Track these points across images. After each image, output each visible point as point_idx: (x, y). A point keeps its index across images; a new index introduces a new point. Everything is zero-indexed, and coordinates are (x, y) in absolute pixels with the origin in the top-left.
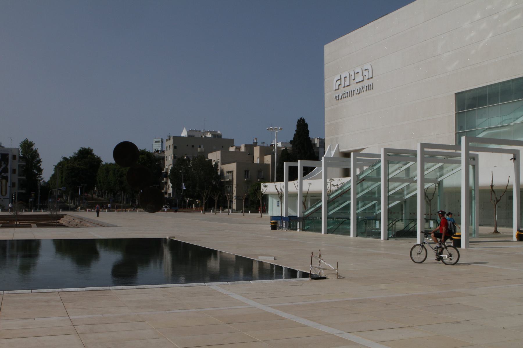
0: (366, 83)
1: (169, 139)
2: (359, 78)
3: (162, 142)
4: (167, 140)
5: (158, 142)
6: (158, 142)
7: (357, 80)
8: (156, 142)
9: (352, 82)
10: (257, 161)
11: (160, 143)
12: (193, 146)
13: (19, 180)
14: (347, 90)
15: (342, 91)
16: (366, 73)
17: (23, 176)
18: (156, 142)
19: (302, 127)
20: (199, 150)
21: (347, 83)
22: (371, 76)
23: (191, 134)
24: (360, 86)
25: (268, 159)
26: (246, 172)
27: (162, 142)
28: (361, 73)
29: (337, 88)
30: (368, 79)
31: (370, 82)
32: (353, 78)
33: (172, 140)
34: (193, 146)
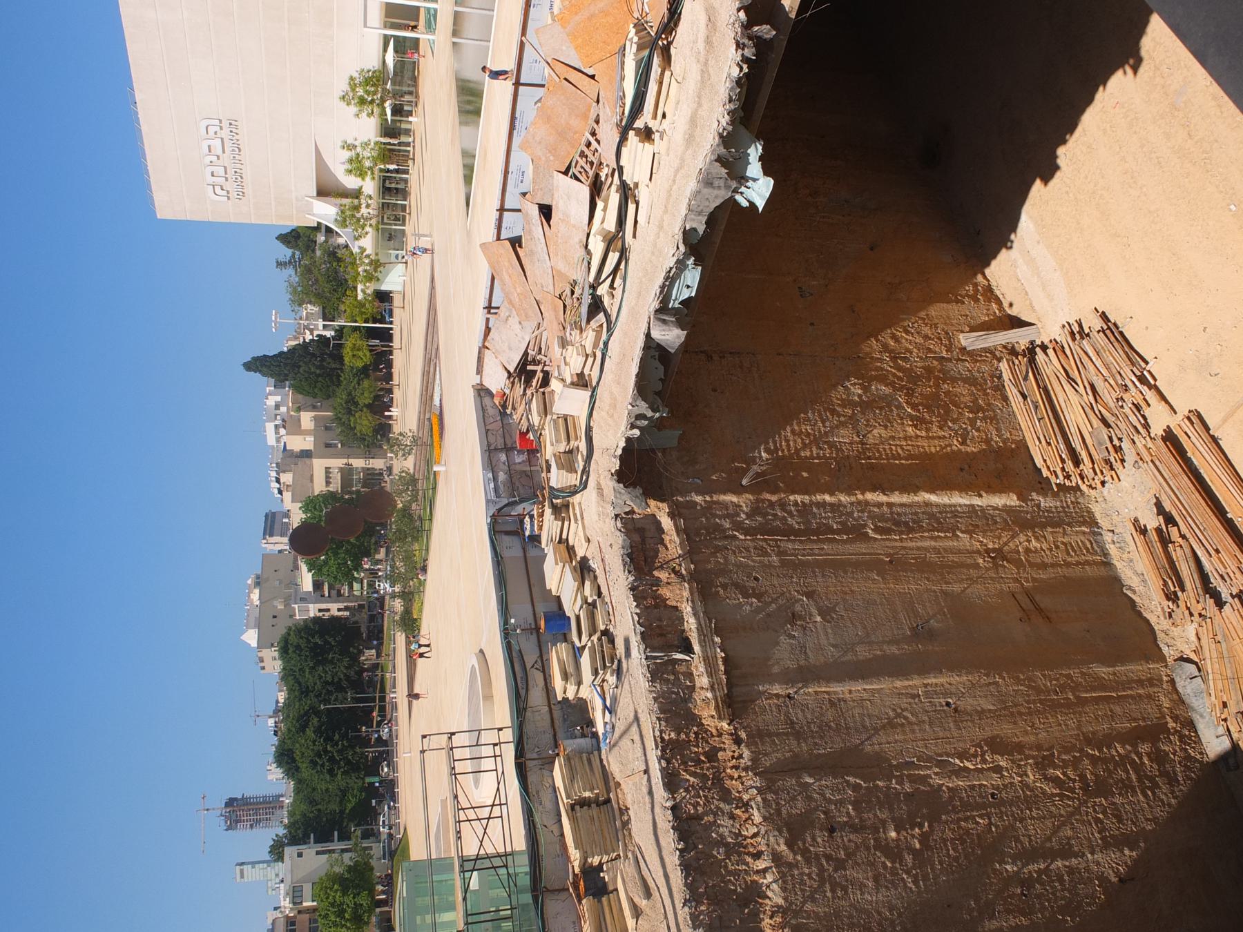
0: (225, 133)
2: (217, 144)
3: (242, 864)
4: (263, 668)
5: (242, 872)
6: (242, 872)
7: (219, 152)
8: (242, 876)
9: (220, 163)
10: (307, 443)
11: (245, 867)
14: (231, 172)
15: (229, 186)
16: (212, 130)
18: (242, 876)
19: (259, 364)
20: (281, 607)
21: (221, 171)
22: (217, 122)
23: (252, 620)
24: (228, 144)
25: (307, 419)
26: (328, 446)
27: (242, 864)
28: (210, 142)
29: (224, 193)
30: (221, 128)
31: (225, 124)
32: (214, 159)
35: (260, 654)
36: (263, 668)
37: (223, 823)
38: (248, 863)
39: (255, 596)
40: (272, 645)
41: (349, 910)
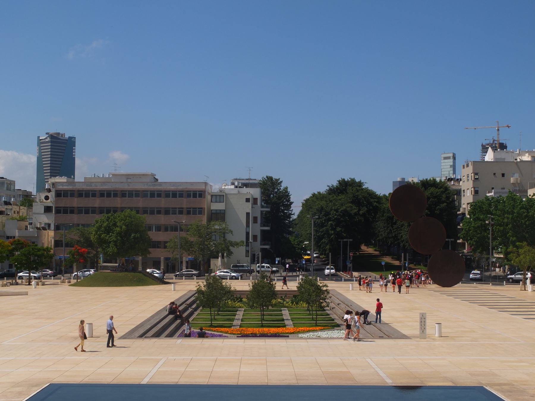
1: (468, 166)
3: (454, 158)
4: (464, 167)
5: (448, 158)
6: (448, 158)
8: (445, 158)
11: (451, 160)
12: (503, 175)
13: (263, 232)
17: (267, 226)
18: (445, 158)
20: (512, 180)
27: (454, 158)
33: (471, 167)
34: (503, 175)
35: (470, 164)
36: (464, 167)
37: (488, 142)
38: (454, 162)
39: (527, 158)
40: (476, 174)
41: (107, 238)
